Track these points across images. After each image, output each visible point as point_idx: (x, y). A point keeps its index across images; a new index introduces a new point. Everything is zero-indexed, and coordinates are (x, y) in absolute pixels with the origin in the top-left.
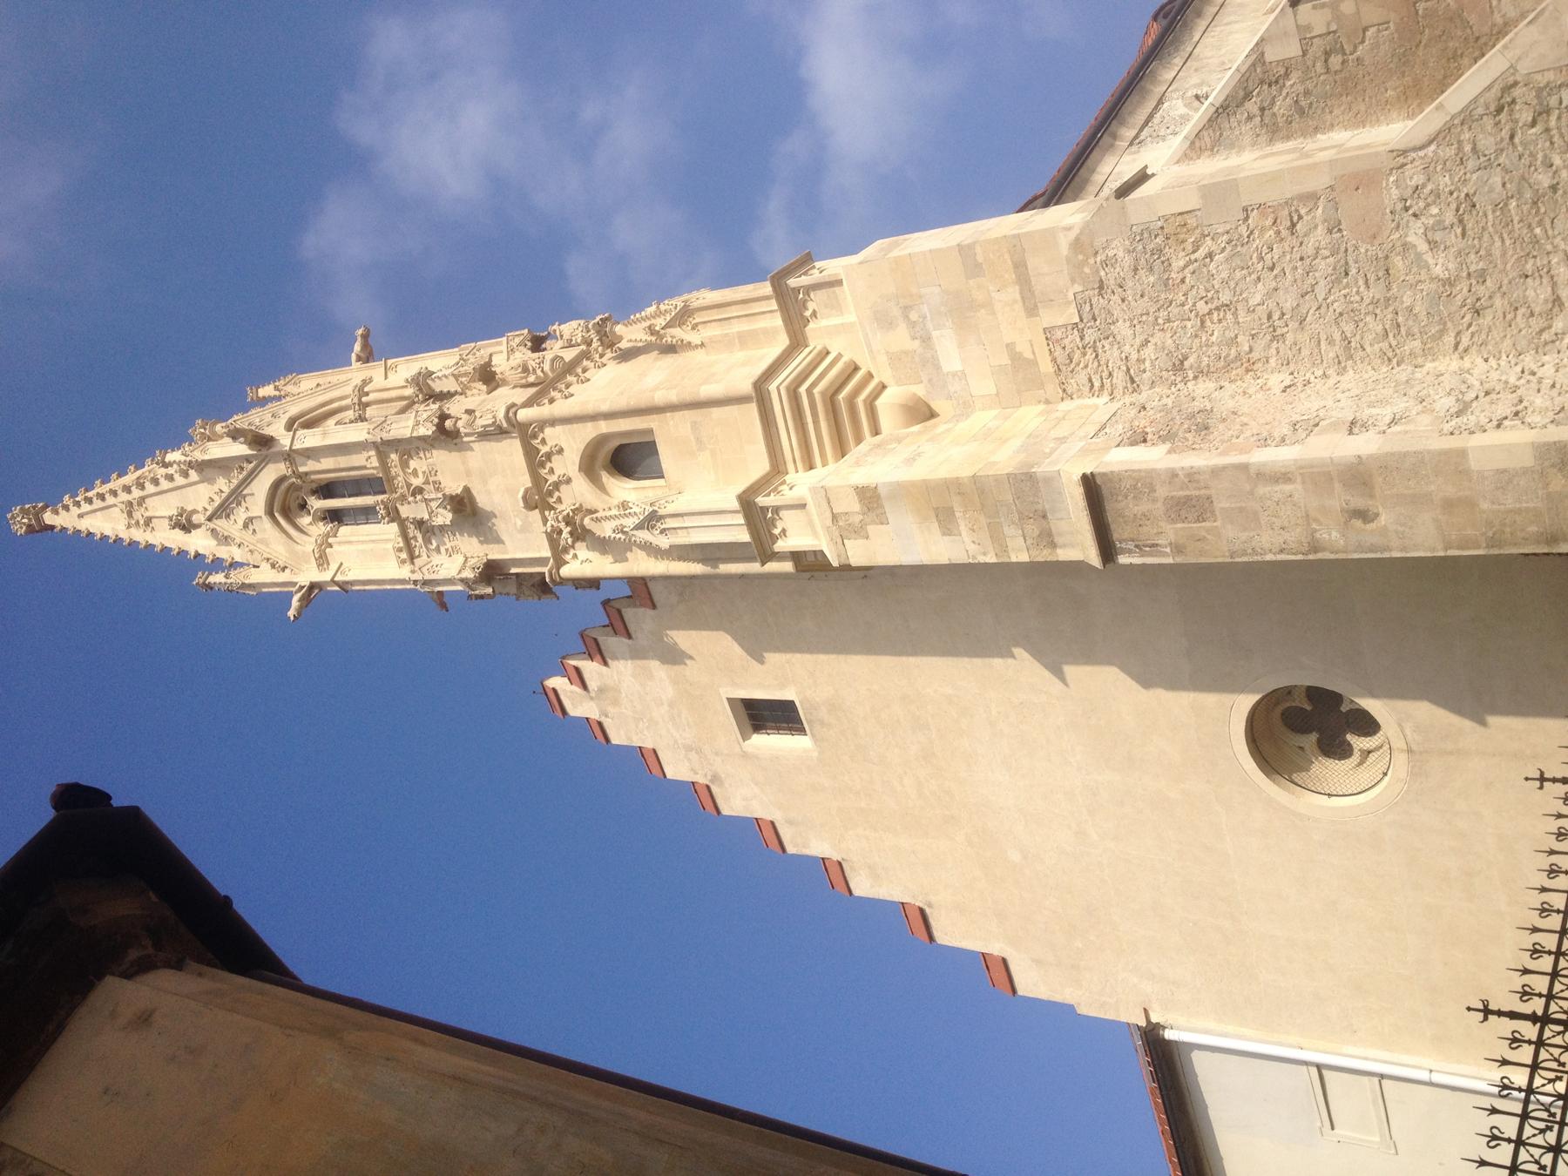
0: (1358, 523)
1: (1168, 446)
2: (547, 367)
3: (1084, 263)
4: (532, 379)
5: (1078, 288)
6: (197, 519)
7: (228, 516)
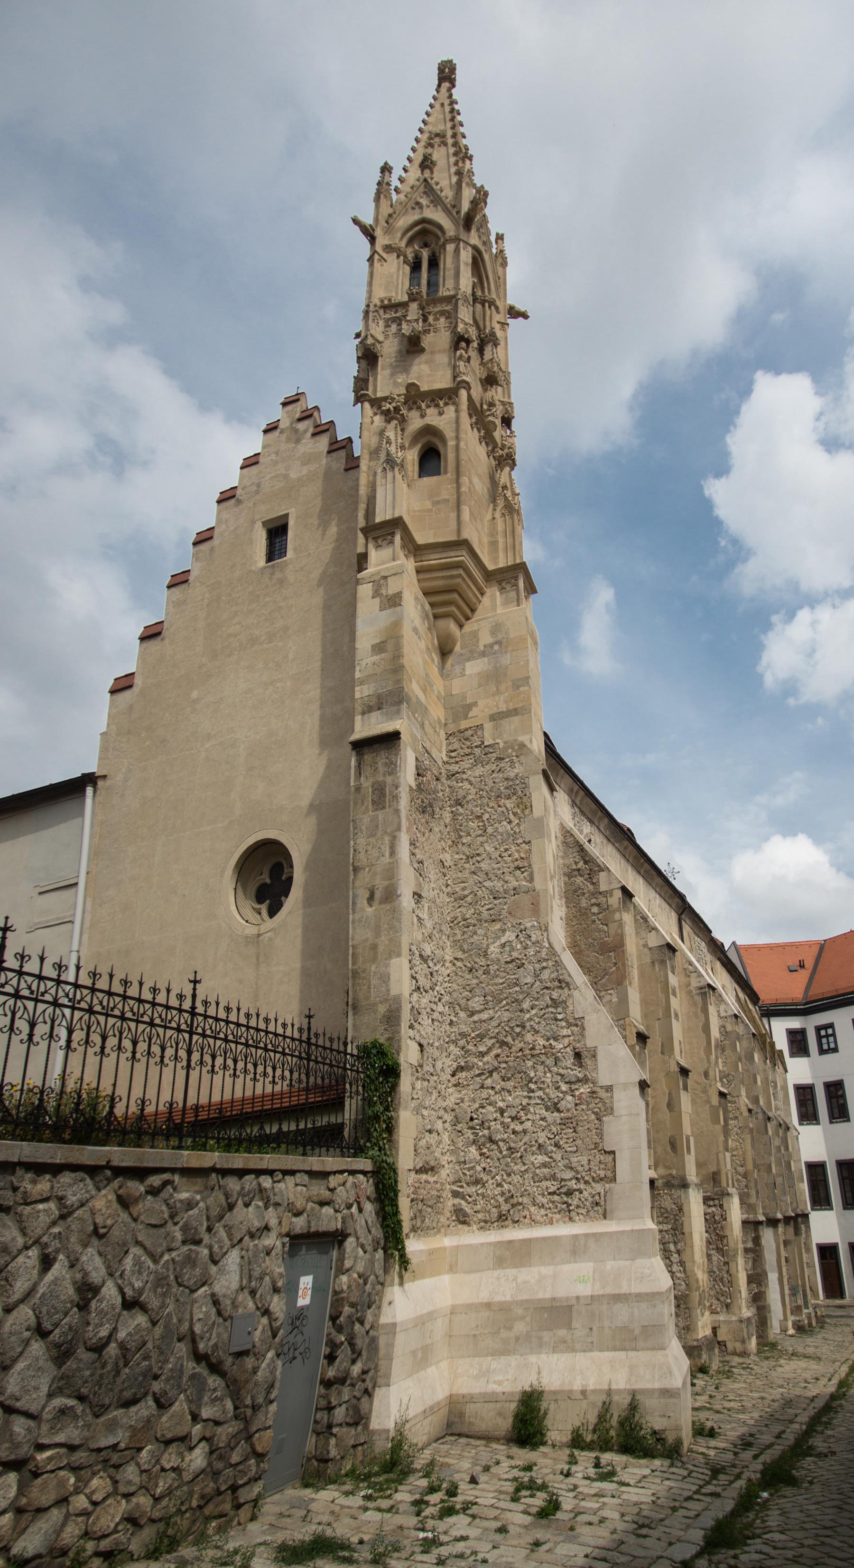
0: (368, 896)
1: (415, 787)
2: (491, 418)
3: (513, 749)
4: (485, 407)
5: (501, 745)
6: (427, 173)
7: (425, 193)
